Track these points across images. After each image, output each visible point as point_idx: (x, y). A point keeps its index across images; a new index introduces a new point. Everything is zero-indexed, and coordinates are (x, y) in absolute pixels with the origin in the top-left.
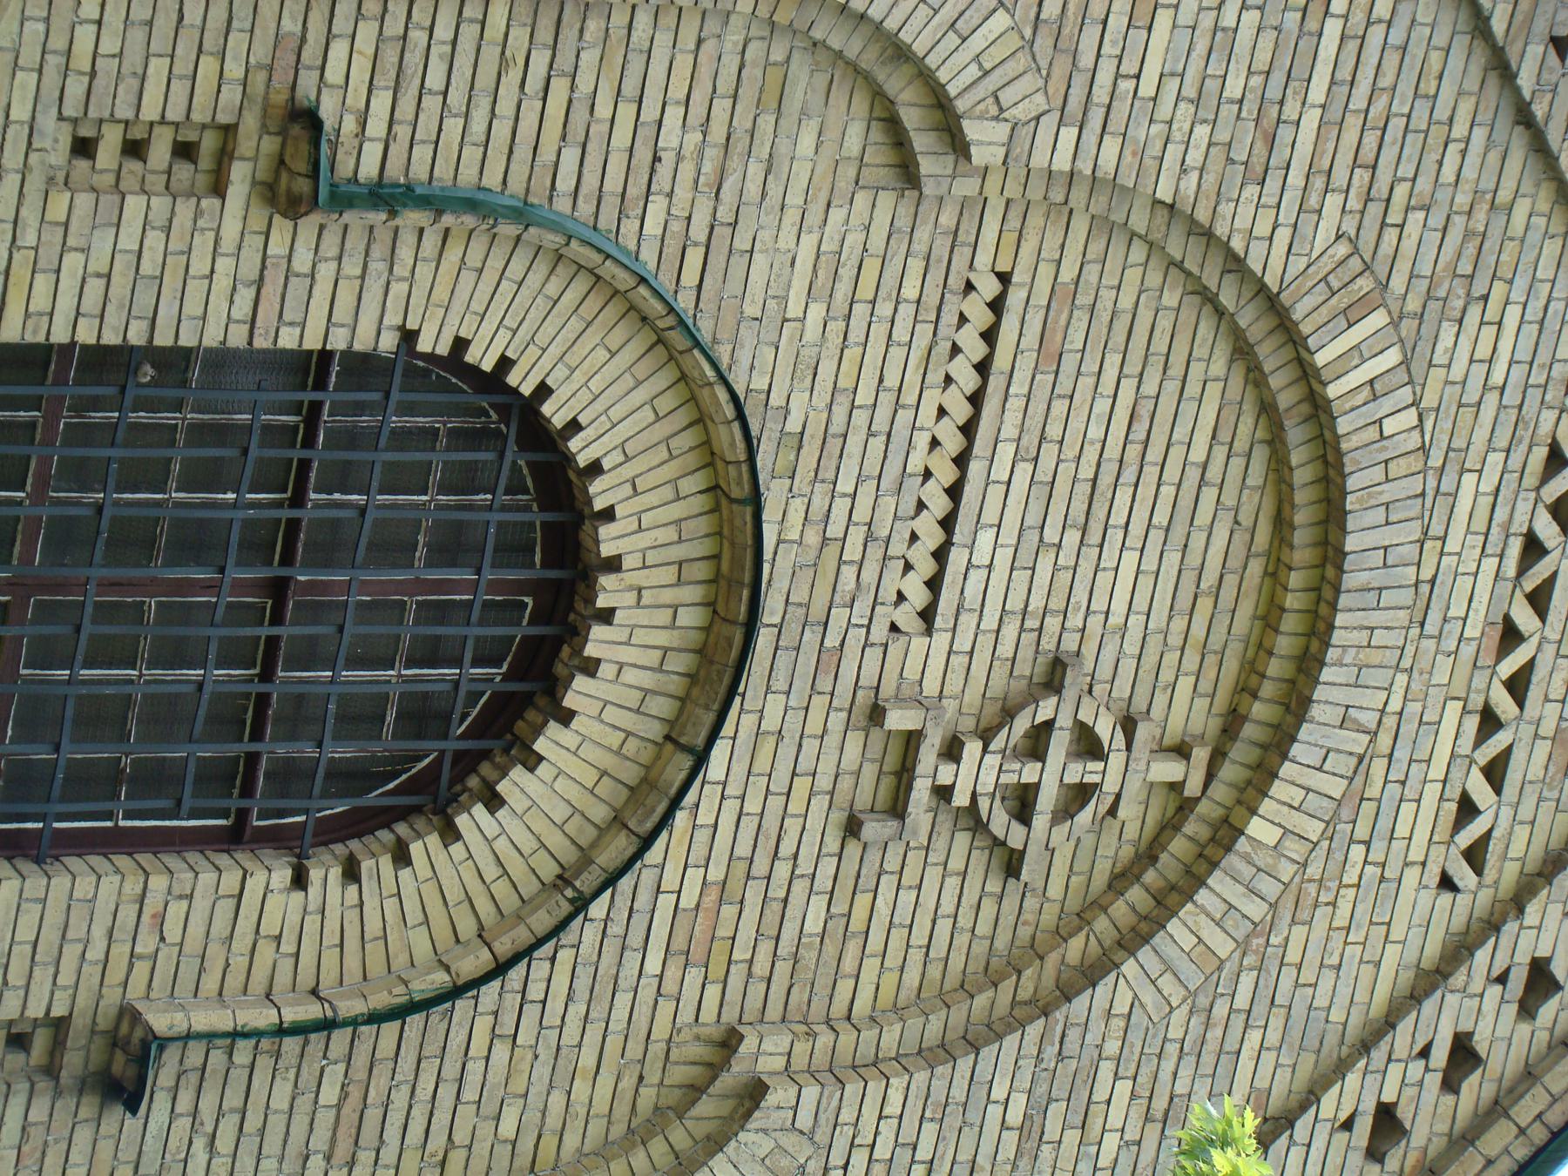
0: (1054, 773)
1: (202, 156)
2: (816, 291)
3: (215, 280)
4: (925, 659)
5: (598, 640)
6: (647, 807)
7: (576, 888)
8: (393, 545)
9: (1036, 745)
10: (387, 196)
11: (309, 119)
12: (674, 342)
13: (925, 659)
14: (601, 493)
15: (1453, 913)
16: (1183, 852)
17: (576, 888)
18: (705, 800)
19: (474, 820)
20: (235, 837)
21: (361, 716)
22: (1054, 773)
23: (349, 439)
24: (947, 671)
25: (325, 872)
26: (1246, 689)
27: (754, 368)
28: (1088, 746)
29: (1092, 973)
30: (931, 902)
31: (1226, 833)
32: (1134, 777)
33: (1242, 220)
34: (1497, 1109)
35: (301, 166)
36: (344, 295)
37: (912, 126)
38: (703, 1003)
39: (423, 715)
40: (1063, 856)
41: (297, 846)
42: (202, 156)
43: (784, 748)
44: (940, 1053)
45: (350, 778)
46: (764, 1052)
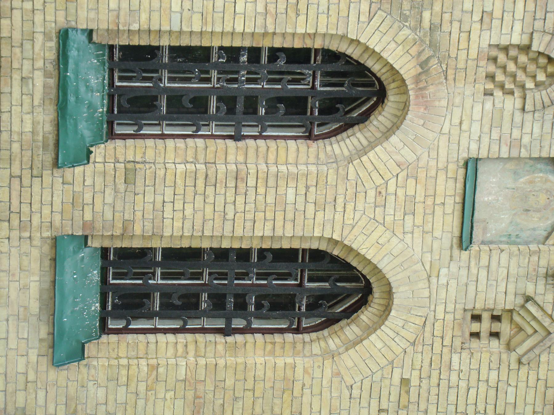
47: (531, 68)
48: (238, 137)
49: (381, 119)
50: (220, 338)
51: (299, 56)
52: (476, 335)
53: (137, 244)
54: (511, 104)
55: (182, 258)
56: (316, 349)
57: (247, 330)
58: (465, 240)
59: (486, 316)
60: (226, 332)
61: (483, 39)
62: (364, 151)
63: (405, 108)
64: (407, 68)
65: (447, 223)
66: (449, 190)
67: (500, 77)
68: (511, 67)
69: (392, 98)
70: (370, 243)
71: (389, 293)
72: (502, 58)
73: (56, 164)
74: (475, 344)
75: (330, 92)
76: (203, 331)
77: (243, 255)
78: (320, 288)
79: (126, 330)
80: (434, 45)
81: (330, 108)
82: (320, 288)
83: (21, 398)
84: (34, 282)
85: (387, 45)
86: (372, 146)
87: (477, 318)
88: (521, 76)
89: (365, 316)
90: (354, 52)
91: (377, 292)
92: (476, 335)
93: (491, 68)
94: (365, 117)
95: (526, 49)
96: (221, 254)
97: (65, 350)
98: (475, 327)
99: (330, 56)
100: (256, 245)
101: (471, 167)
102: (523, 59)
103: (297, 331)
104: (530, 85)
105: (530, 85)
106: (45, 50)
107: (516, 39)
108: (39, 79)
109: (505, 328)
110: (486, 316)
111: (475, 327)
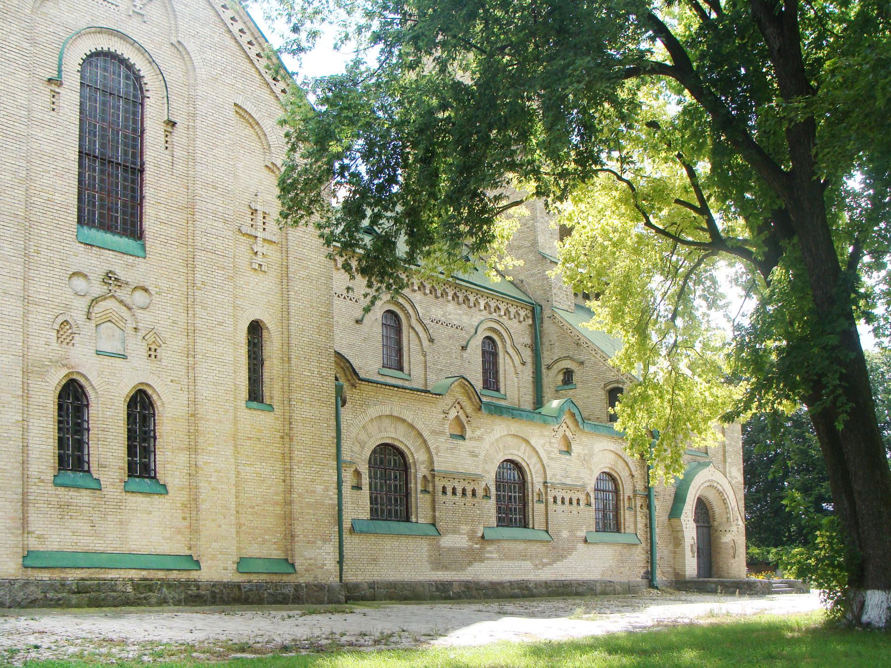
1: (55, 94)
3: (70, 96)
5: (119, 52)
6: (142, 50)
8: (105, 77)
10: (60, 71)
11: (50, 80)
12: (79, 35)
14: (99, 49)
17: (152, 62)
18: (140, 42)
20: (142, 104)
21: (127, 85)
23: (91, 81)
25: (147, 94)
35: (55, 81)
39: (127, 78)
42: (55, 94)
43: (131, 28)
46: (174, 40)
47: (64, 330)
48: (88, 430)
49: (82, 381)
50: (157, 440)
51: (60, 407)
52: (156, 356)
53: (126, 465)
55: (131, 451)
56: (161, 409)
57: (154, 430)
58: (124, 357)
59: (150, 353)
60: (155, 438)
61: (55, 345)
62: (94, 388)
63: (78, 373)
64: (65, 371)
65: (119, 362)
67: (68, 341)
68: (64, 337)
69: (75, 377)
71: (142, 384)
72: (60, 340)
74: (158, 357)
75: (73, 399)
76: (155, 445)
77: (129, 430)
78: (141, 406)
79: (155, 470)
80: (57, 362)
81: (77, 398)
82: (141, 406)
85: (56, 378)
86: (92, 385)
87: (150, 356)
88: (67, 334)
89: (150, 392)
90: (59, 389)
91: (141, 387)
92: (156, 356)
93: (65, 343)
94: (81, 387)
95: (58, 331)
96: (129, 438)
98: (153, 356)
99: (60, 397)
100: (126, 426)
101: (98, 353)
102: (61, 333)
103: (154, 415)
104: (70, 331)
105: (70, 331)
107: (55, 334)
110: (150, 353)
111: (153, 356)
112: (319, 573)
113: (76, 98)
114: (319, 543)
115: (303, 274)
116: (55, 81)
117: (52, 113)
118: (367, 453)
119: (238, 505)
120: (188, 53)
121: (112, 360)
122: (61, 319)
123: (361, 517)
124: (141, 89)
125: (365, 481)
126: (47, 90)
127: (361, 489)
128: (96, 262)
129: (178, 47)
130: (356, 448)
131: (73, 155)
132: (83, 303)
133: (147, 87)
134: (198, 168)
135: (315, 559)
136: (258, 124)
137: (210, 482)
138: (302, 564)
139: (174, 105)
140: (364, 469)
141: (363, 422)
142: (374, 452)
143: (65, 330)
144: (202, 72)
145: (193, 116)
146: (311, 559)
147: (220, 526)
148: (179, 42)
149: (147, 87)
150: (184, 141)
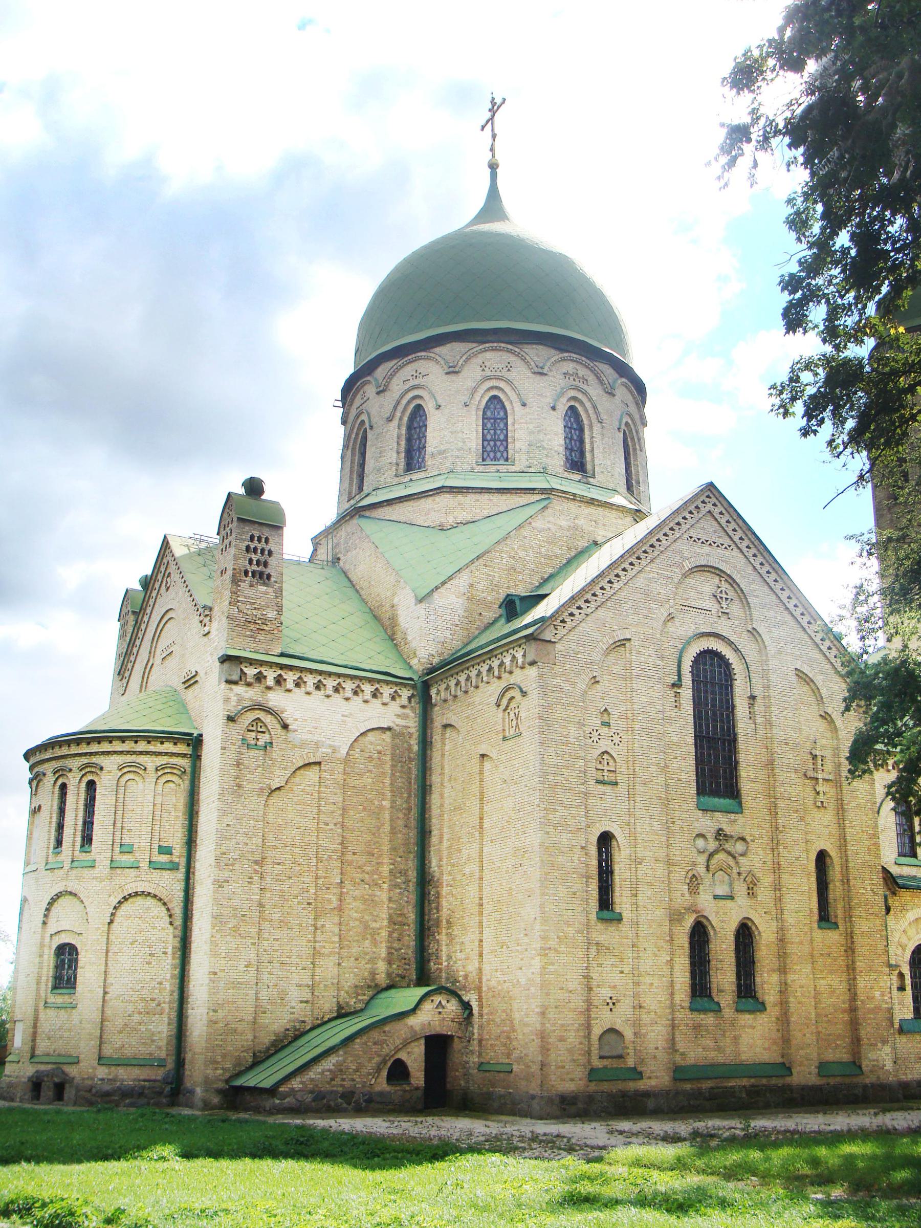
0: (724, 596)
1: (677, 694)
2: (685, 627)
3: (687, 693)
4: (714, 611)
6: (730, 643)
7: (737, 650)
9: (721, 598)
13: (714, 611)
15: (735, 549)
16: (732, 581)
17: (737, 650)
19: (730, 661)
20: (731, 686)
21: (720, 673)
22: (724, 596)
24: (714, 607)
25: (736, 677)
26: (715, 573)
27: (691, 634)
28: (721, 592)
29: (742, 590)
30: (735, 609)
31: (729, 576)
32: (725, 586)
33: (676, 580)
34: (753, 543)
35: (677, 685)
36: (687, 679)
37: (671, 618)
38: (745, 635)
39: (720, 666)
40: (731, 594)
41: (732, 680)
42: (677, 694)
43: (722, 627)
44: (750, 608)
45: (726, 675)
49: (704, 921)
54: (701, 887)
58: (732, 898)
62: (713, 927)
64: (695, 916)
65: (729, 903)
66: (722, 903)
70: (734, 925)
71: (744, 918)
73: (720, 1011)
75: (700, 935)
83: (774, 1019)
84: (747, 1016)
85: (689, 921)
97: (761, 1007)
106: (695, 1015)
108: (702, 1016)
109: (751, 886)
112: (880, 1073)
113: (690, 692)
114: (879, 1044)
115: (853, 804)
116: (677, 685)
117: (676, 710)
118: (908, 954)
119: (817, 1015)
120: (760, 635)
121: (724, 902)
122: (690, 875)
123: (907, 1017)
124: (730, 672)
125: (908, 981)
126: (671, 693)
127: (905, 990)
128: (708, 823)
129: (754, 633)
130: (899, 952)
131: (691, 740)
132: (702, 859)
133: (735, 671)
134: (774, 731)
135: (877, 1061)
136: (812, 681)
137: (796, 997)
138: (867, 1066)
139: (753, 681)
140: (906, 970)
141: (904, 927)
142: (913, 952)
143: (694, 883)
144: (771, 649)
145: (767, 687)
146: (874, 1061)
147: (804, 1035)
148: (753, 628)
149: (735, 671)
150: (762, 708)
